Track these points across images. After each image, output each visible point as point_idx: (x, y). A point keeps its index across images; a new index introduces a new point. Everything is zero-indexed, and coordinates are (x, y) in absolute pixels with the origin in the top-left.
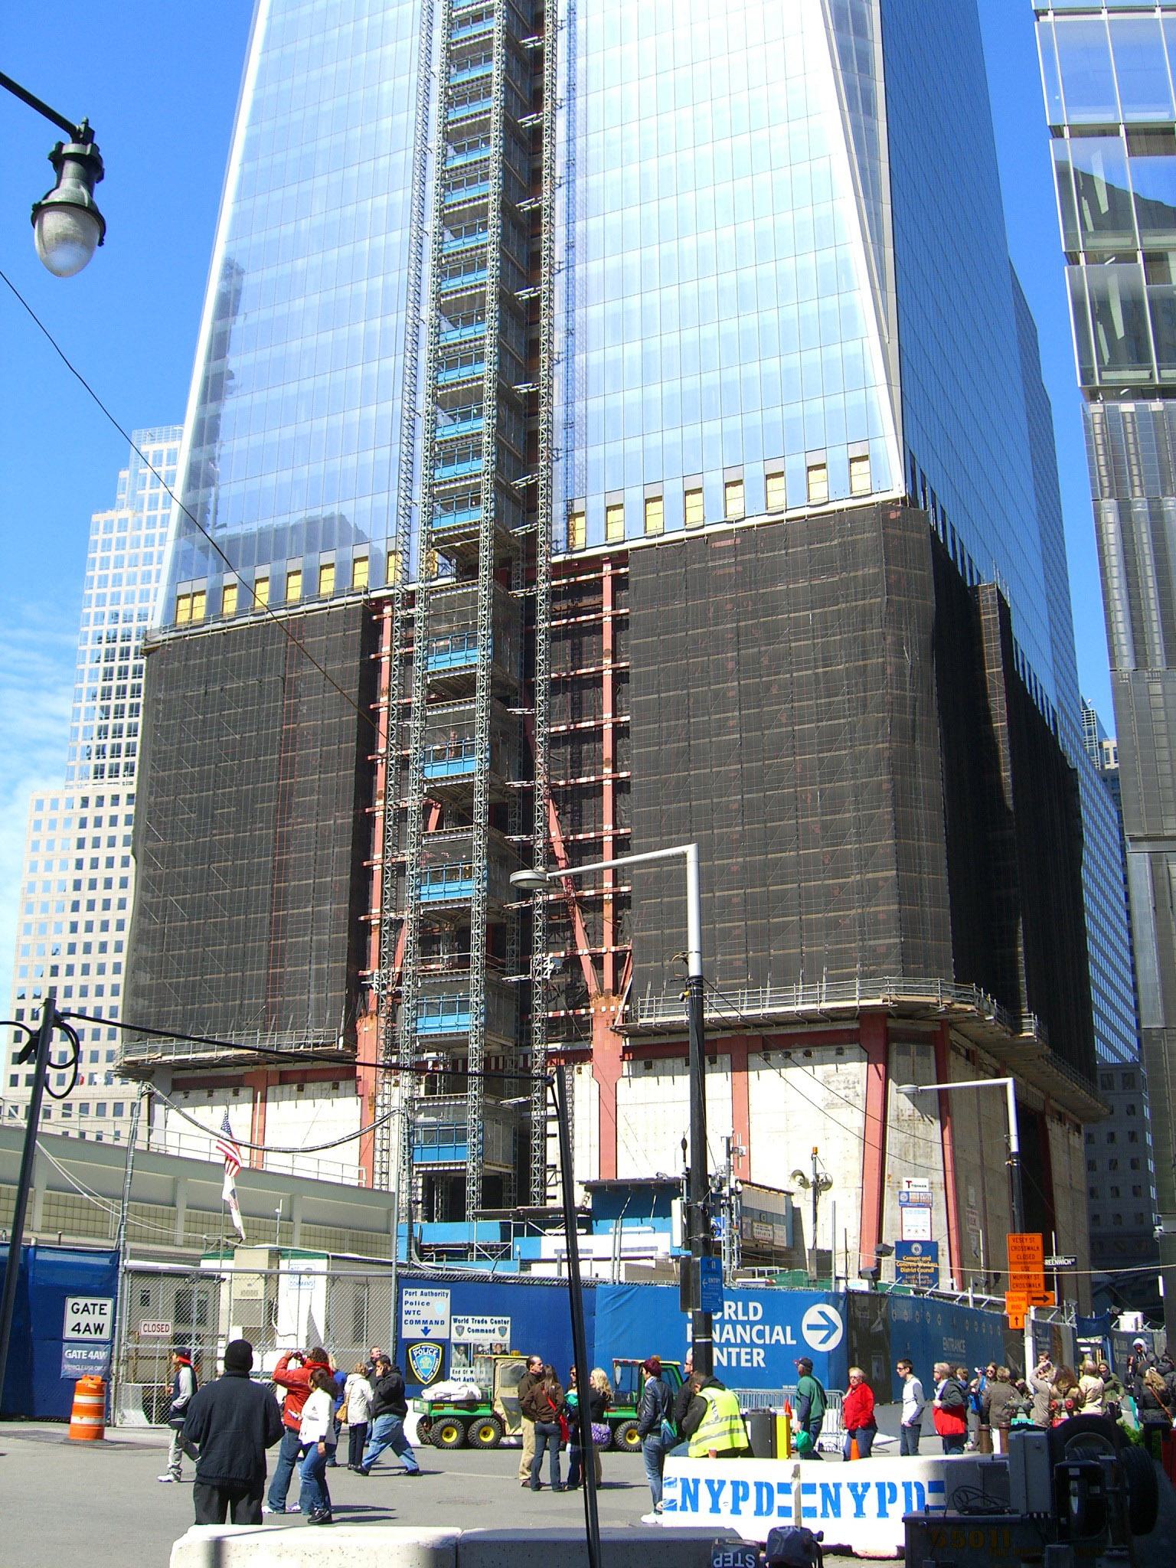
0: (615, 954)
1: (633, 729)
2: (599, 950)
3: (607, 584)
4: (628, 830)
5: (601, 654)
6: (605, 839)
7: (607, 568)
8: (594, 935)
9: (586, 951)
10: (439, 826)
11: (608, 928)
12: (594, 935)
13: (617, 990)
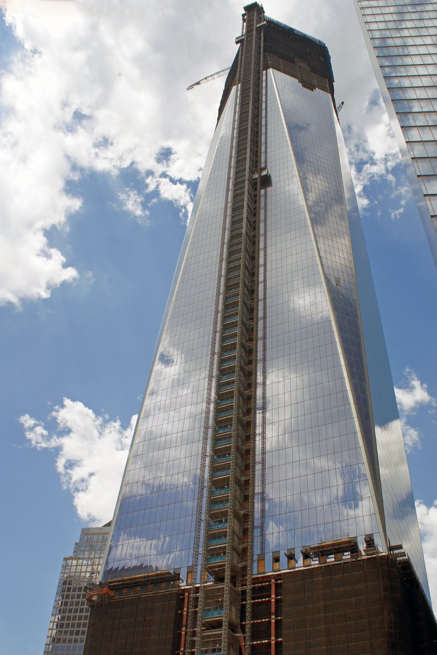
1: (284, 644)
7: (273, 581)
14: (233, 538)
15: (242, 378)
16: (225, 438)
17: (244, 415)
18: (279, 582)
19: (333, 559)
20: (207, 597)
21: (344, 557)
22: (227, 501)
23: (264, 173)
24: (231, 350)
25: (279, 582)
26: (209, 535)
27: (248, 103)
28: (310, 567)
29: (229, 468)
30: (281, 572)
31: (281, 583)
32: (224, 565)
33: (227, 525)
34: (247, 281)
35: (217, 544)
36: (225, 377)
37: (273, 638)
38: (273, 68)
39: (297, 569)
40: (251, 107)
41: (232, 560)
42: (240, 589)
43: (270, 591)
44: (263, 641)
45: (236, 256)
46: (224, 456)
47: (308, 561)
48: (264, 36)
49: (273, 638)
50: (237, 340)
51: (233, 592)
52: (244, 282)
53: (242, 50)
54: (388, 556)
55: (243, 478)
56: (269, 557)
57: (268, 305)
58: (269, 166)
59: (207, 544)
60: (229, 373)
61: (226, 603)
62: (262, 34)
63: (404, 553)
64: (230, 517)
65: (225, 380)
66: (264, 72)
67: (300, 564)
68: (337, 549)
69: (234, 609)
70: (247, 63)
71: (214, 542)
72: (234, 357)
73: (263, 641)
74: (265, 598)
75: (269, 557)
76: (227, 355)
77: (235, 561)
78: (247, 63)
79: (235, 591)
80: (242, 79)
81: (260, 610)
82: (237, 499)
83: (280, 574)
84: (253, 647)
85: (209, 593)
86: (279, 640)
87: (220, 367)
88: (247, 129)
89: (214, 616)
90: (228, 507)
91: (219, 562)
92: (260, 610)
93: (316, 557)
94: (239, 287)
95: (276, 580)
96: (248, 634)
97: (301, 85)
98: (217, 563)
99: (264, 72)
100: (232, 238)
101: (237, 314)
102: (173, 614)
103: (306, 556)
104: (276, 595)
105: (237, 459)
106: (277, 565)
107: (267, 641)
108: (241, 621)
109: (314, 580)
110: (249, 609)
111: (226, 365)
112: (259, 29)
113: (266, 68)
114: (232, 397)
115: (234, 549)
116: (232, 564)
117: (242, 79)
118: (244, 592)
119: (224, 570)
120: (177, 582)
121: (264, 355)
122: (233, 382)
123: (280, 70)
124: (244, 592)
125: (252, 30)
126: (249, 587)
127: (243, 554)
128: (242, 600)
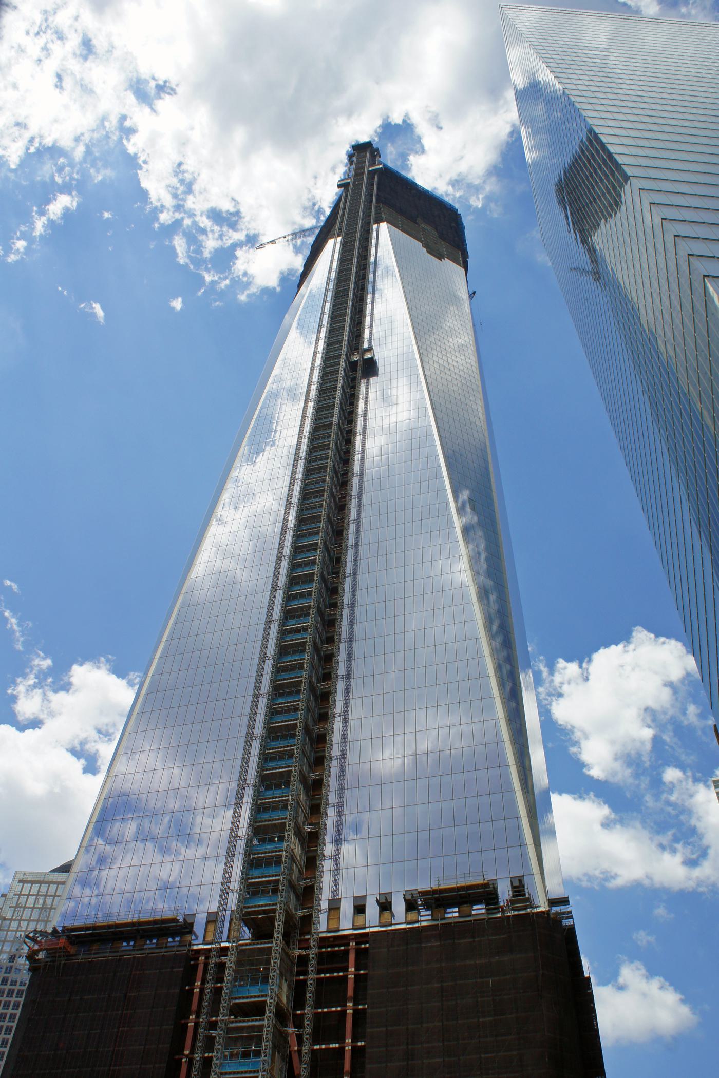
3: (352, 957)
7: (353, 944)
15: (313, 704)
16: (286, 712)
17: (315, 723)
18: (363, 946)
19: (457, 914)
20: (239, 963)
21: (474, 912)
23: (368, 356)
24: (304, 582)
25: (363, 946)
26: (251, 861)
28: (416, 925)
29: (291, 756)
30: (367, 930)
31: (366, 949)
32: (274, 911)
36: (293, 621)
37: (348, 1041)
39: (393, 927)
41: (287, 904)
42: (297, 952)
44: (331, 1046)
45: (309, 556)
46: (278, 786)
47: (412, 916)
48: (379, 184)
49: (348, 1041)
50: (312, 602)
52: (332, 490)
53: (346, 196)
55: (313, 776)
56: (347, 908)
57: (359, 586)
58: (374, 343)
59: (247, 875)
60: (300, 616)
62: (376, 179)
65: (292, 624)
66: (375, 226)
67: (400, 917)
68: (464, 896)
70: (354, 212)
73: (331, 1046)
74: (338, 972)
75: (347, 908)
76: (297, 590)
77: (292, 905)
78: (354, 212)
79: (287, 954)
80: (344, 230)
81: (331, 991)
82: (294, 861)
83: (366, 934)
84: (313, 1052)
86: (359, 1044)
87: (286, 606)
88: (348, 290)
89: (252, 993)
90: (286, 817)
91: (266, 905)
92: (331, 991)
94: (323, 496)
95: (357, 944)
96: (308, 1030)
97: (425, 250)
99: (375, 226)
100: (316, 429)
101: (318, 533)
102: (177, 991)
103: (411, 906)
105: (304, 745)
107: (337, 1045)
108: (295, 1009)
109: (424, 945)
111: (295, 604)
112: (372, 174)
113: (378, 221)
114: (303, 651)
117: (344, 230)
118: (303, 960)
119: (272, 920)
120: (188, 938)
121: (349, 668)
122: (305, 629)
123: (398, 228)
125: (363, 173)
126: (313, 952)
127: (308, 894)
128: (298, 974)
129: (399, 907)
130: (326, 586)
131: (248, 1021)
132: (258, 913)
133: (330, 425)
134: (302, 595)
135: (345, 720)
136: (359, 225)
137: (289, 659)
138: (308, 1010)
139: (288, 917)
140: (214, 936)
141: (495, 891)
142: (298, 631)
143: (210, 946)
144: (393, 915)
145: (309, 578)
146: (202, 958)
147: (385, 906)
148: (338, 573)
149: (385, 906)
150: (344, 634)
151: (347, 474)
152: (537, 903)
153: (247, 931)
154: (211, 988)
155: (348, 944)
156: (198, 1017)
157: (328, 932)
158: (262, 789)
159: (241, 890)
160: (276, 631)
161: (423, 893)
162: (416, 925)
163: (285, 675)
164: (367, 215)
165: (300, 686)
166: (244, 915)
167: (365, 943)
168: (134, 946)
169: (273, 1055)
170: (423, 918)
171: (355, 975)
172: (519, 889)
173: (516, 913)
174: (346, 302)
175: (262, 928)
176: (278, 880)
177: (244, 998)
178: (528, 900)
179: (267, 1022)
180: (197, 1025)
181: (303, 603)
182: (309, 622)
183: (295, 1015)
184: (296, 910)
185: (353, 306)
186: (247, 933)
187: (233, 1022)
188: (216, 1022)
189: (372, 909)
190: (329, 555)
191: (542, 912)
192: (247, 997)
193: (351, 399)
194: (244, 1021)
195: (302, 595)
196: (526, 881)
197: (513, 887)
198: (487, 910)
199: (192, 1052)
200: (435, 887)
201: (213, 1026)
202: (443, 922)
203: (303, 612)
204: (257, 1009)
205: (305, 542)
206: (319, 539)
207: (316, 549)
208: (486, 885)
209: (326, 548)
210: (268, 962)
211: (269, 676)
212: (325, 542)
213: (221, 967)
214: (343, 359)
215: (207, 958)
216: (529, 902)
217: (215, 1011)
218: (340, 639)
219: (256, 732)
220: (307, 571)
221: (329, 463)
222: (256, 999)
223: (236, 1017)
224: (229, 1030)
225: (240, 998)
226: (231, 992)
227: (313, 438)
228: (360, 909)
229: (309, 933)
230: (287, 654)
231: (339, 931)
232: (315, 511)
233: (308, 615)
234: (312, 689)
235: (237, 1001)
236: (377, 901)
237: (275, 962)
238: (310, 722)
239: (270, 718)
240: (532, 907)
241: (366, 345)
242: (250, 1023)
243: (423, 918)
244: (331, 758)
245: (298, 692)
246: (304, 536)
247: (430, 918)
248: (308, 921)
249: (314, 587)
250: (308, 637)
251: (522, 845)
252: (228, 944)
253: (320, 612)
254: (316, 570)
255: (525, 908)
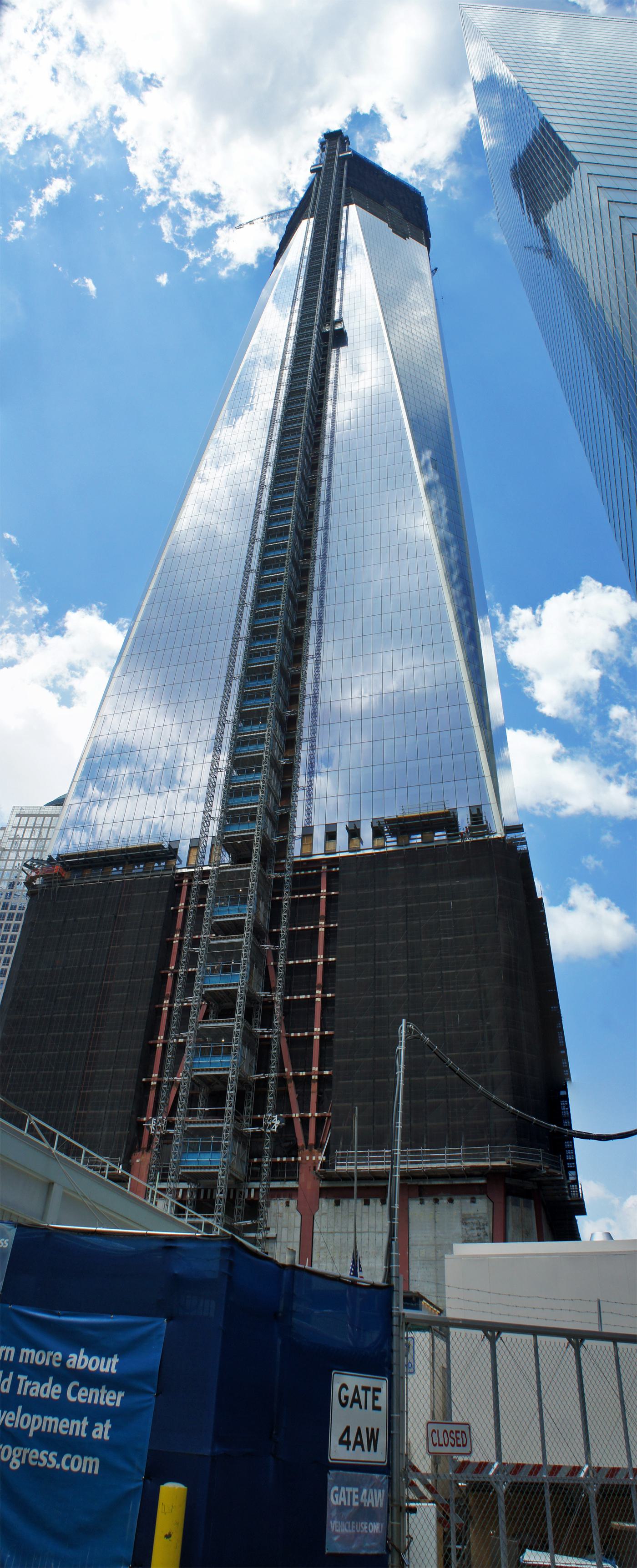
0: (317, 1118)
1: (338, 966)
2: (306, 1115)
3: (324, 880)
4: (331, 1033)
5: (317, 919)
6: (315, 1037)
7: (324, 868)
8: (304, 1106)
9: (297, 1115)
10: (206, 1016)
11: (314, 1098)
12: (304, 1106)
13: (318, 1145)
14: (268, 798)
15: (287, 647)
16: (263, 654)
17: (290, 665)
19: (420, 841)
20: (219, 885)
21: (436, 839)
22: (262, 741)
23: (338, 327)
24: (280, 535)
26: (231, 790)
27: (317, 289)
28: (382, 850)
30: (338, 855)
31: (336, 872)
33: (260, 776)
34: (299, 527)
35: (243, 804)
36: (270, 571)
37: (320, 956)
38: (357, 204)
39: (361, 853)
40: (326, 243)
41: (264, 830)
42: (273, 876)
43: (320, 882)
44: (304, 961)
45: (284, 512)
46: (255, 722)
47: (379, 842)
48: (348, 169)
49: (320, 956)
50: (287, 553)
51: (262, 879)
52: (305, 450)
53: (318, 180)
54: (504, 838)
55: (288, 713)
56: (319, 835)
57: (330, 539)
58: (344, 316)
59: (227, 803)
60: (276, 566)
61: (252, 895)
62: (346, 165)
63: (524, 839)
64: (265, 765)
65: (269, 574)
66: (345, 208)
67: (367, 842)
69: (262, 906)
70: (325, 195)
71: (236, 801)
72: (285, 546)
75: (319, 835)
76: (273, 543)
78: (325, 195)
79: (264, 877)
80: (316, 211)
81: (304, 910)
83: (337, 858)
85: (223, 878)
88: (320, 267)
89: (230, 913)
90: (264, 750)
91: (245, 832)
93: (392, 837)
94: (297, 456)
95: (328, 868)
96: (282, 947)
97: (391, 230)
98: (241, 832)
99: (345, 208)
101: (292, 490)
103: (378, 833)
104: (329, 889)
105: (280, 685)
106: (331, 846)
107: (310, 961)
108: (271, 927)
109: (390, 869)
110: (286, 907)
111: (271, 556)
112: (342, 160)
113: (348, 203)
114: (279, 598)
115: (268, 813)
116: (264, 836)
117: (316, 211)
118: (279, 883)
119: (250, 845)
120: (173, 862)
121: (321, 615)
122: (281, 578)
123: (366, 209)
124: (279, 883)
125: (334, 159)
126: (288, 875)
127: (283, 822)
128: (275, 895)
129: (367, 834)
130: (300, 538)
131: (228, 938)
132: (238, 838)
133: (303, 391)
134: (278, 547)
135: (318, 662)
136: (331, 207)
137: (267, 606)
138: (283, 927)
139: (265, 842)
140: (197, 860)
141: (455, 819)
142: (274, 580)
143: (192, 870)
144: (361, 842)
145: (284, 532)
146: (186, 881)
147: (354, 832)
148: (311, 526)
149: (354, 832)
150: (316, 583)
151: (319, 436)
152: (494, 830)
153: (227, 855)
154: (194, 909)
155: (320, 868)
156: (182, 935)
157: (302, 856)
158: (241, 725)
159: (221, 818)
160: (254, 580)
161: (389, 821)
162: (382, 850)
163: (263, 621)
164: (338, 197)
165: (276, 631)
166: (224, 841)
167: (336, 867)
168: (123, 871)
169: (251, 969)
170: (388, 844)
171: (327, 896)
172: (477, 816)
173: (474, 839)
174: (318, 278)
175: (239, 851)
176: (256, 808)
177: (224, 917)
178: (486, 827)
179: (245, 940)
180: (181, 942)
181: (278, 554)
182: (284, 572)
183: (271, 933)
184: (272, 837)
185: (324, 281)
186: (227, 858)
187: (214, 939)
188: (199, 939)
189: (342, 836)
190: (303, 510)
191: (499, 838)
192: (227, 917)
193: (323, 367)
194: (224, 939)
195: (278, 547)
196: (484, 810)
197: (472, 815)
198: (448, 836)
199: (177, 967)
200: (400, 815)
201: (196, 943)
202: (408, 847)
203: (279, 563)
204: (237, 928)
205: (280, 498)
206: (294, 496)
207: (291, 505)
208: (447, 814)
209: (300, 504)
210: (247, 883)
211: (247, 622)
212: (299, 499)
213: (204, 888)
214: (315, 330)
215: (190, 881)
216: (486, 829)
217: (198, 930)
218: (313, 588)
219: (235, 673)
220: (283, 525)
221: (303, 425)
222: (236, 918)
223: (217, 935)
224: (211, 947)
225: (221, 917)
226: (213, 912)
227: (288, 402)
228: (331, 835)
229: (284, 858)
230: (264, 601)
231: (312, 855)
232: (290, 469)
233: (283, 565)
234: (287, 633)
235: (218, 920)
236: (347, 828)
237: (253, 884)
238: (285, 664)
239: (249, 660)
240: (489, 833)
241: (336, 317)
242: (230, 941)
243: (388, 844)
244: (304, 697)
245: (274, 636)
246: (279, 493)
247: (395, 844)
248: (283, 847)
249: (288, 540)
250: (283, 586)
251: (480, 777)
252: (209, 868)
253: (294, 563)
254: (291, 524)
255: (483, 835)
